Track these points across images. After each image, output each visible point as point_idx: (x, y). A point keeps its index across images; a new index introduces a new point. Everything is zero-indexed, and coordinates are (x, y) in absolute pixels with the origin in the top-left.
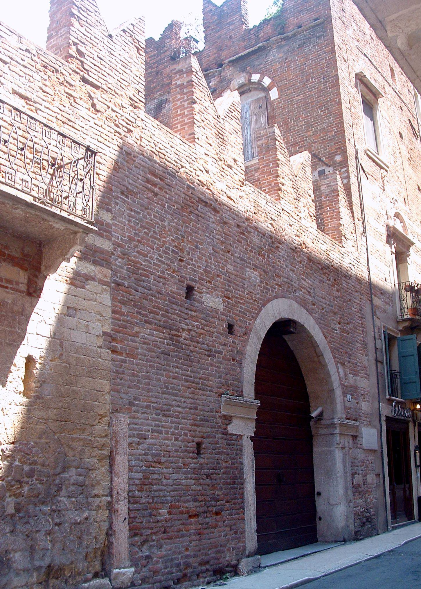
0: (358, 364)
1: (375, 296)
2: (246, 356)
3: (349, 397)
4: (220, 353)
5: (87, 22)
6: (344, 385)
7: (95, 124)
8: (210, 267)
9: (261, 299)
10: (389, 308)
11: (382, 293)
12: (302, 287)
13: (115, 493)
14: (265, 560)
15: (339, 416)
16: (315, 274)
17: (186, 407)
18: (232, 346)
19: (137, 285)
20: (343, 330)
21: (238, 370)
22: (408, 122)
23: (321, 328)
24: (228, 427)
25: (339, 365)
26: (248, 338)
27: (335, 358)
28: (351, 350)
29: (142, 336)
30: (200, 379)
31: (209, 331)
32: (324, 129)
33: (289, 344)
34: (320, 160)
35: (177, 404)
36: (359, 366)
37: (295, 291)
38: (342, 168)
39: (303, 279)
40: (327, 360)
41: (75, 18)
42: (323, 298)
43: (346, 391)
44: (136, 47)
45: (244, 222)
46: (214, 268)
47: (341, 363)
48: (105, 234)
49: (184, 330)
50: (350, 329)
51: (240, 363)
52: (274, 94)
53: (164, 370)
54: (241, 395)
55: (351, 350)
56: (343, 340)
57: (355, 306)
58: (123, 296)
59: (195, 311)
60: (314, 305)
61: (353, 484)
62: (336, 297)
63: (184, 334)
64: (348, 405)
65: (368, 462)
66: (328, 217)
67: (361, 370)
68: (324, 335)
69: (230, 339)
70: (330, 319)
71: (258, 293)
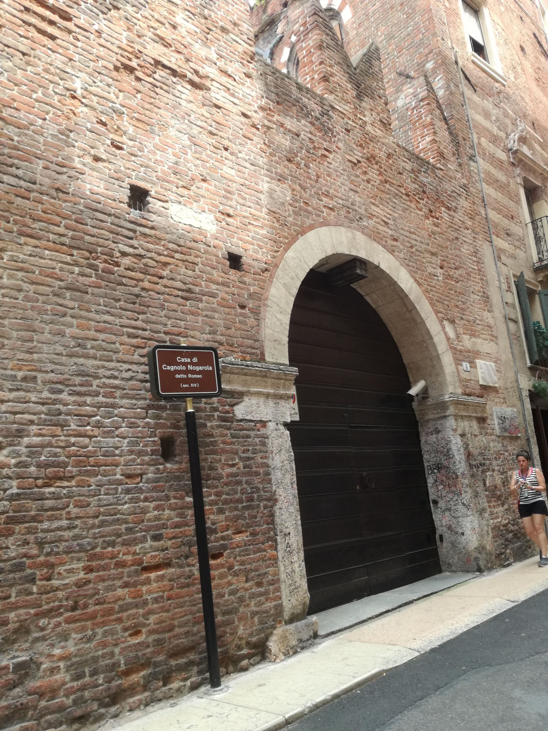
0: (478, 322)
1: (498, 236)
2: (269, 302)
3: (466, 365)
4: (214, 296)
6: (455, 349)
8: (185, 166)
9: (296, 225)
10: (521, 254)
11: (508, 234)
12: (371, 216)
14: (324, 620)
15: (452, 389)
16: (394, 200)
17: (131, 378)
18: (238, 287)
20: (449, 277)
21: (251, 321)
22: (533, 36)
23: (410, 272)
24: (235, 408)
25: (446, 323)
26: (271, 277)
27: (437, 312)
28: (464, 303)
29: (12, 256)
30: (166, 333)
31: (186, 261)
32: (409, 35)
33: (367, 298)
34: (408, 77)
35: (108, 373)
36: (478, 324)
37: (361, 218)
39: (374, 204)
40: (423, 315)
42: (410, 233)
43: (461, 357)
45: (256, 112)
46: (193, 168)
47: (448, 319)
49: (124, 254)
50: (461, 275)
51: (256, 312)
53: (73, 317)
54: (262, 359)
55: (464, 303)
56: (451, 289)
57: (466, 247)
59: (152, 228)
60: (396, 240)
61: (485, 484)
62: (433, 233)
63: (126, 261)
64: (464, 375)
65: (506, 454)
66: (417, 136)
67: (483, 329)
68: (416, 280)
69: (233, 275)
70: (424, 261)
71: (289, 216)
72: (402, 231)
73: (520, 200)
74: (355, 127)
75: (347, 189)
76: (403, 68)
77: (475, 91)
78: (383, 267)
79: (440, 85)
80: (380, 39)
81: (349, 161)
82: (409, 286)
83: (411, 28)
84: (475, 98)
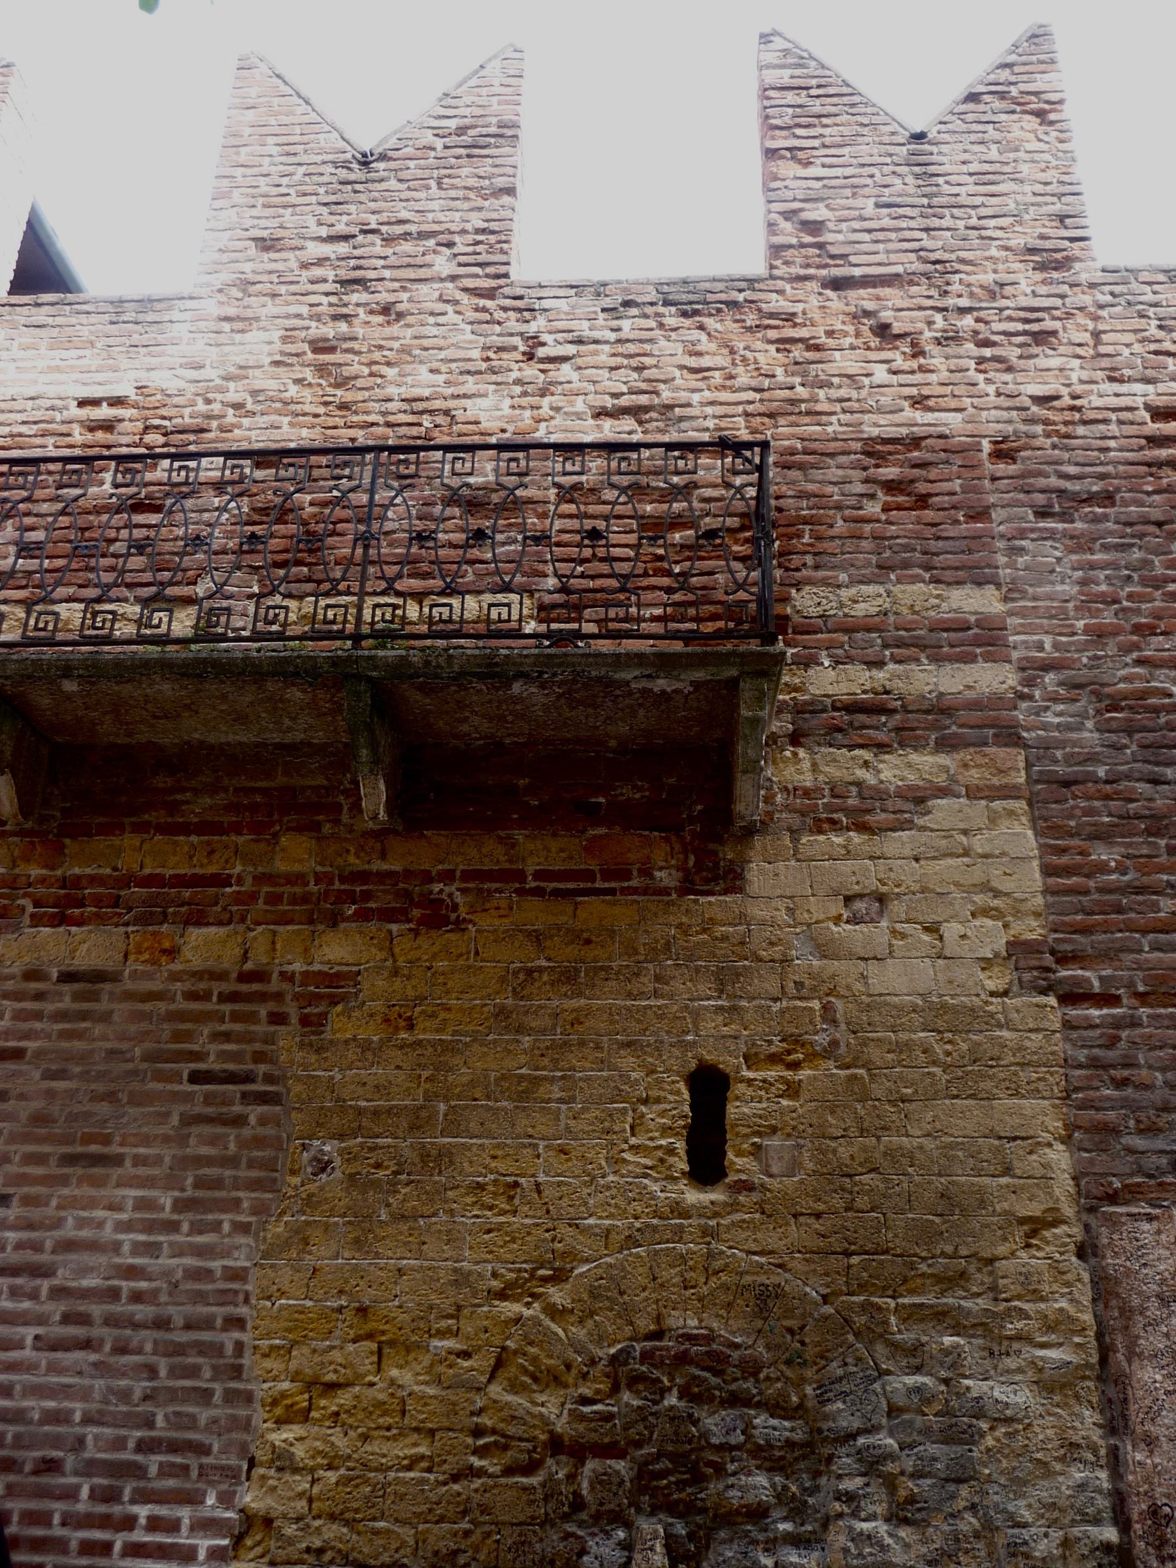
5: (824, 146)
7: (895, 373)
13: (1137, 1508)
19: (1157, 764)
41: (783, 157)
44: (1032, 113)
48: (978, 651)
58: (1089, 812)
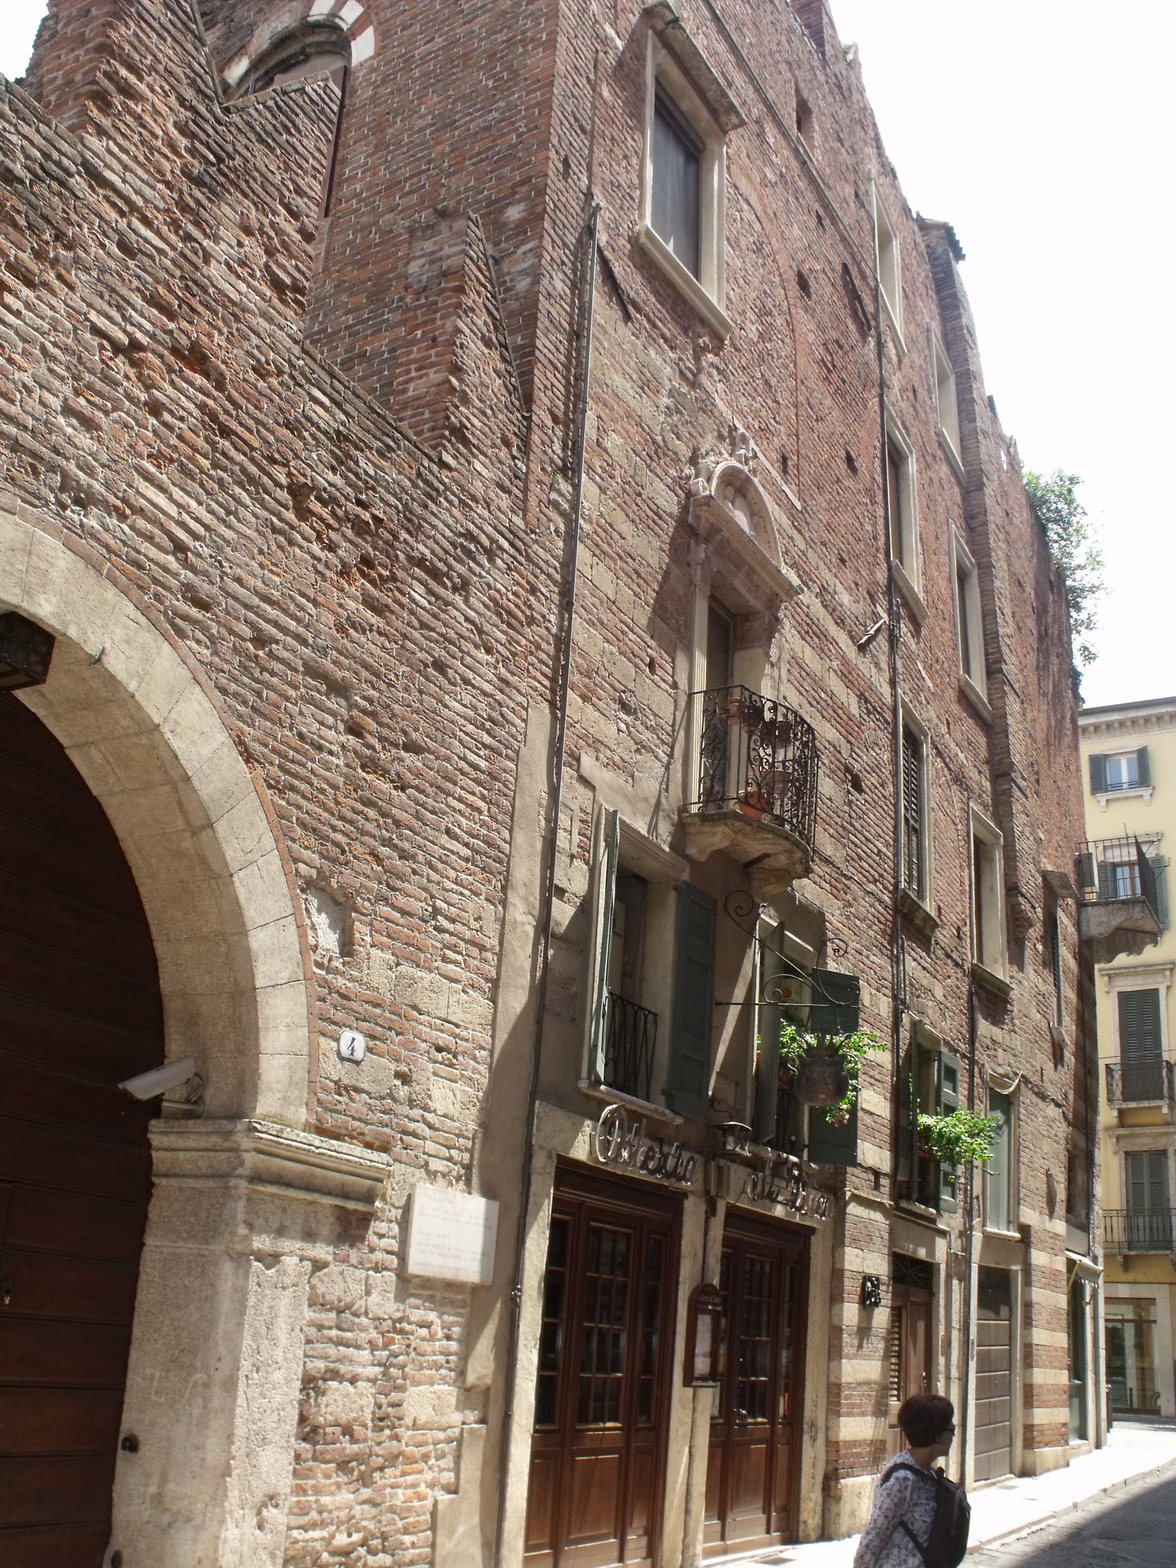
1: (585, 698)
3: (353, 1040)
11: (625, 707)
32: (487, 128)
38: (523, 243)
40: (231, 853)
52: (363, 48)
66: (410, 362)
68: (240, 743)
72: (235, 587)
73: (689, 626)
74: (160, 251)
75: (55, 403)
76: (452, 203)
77: (627, 317)
78: (115, 664)
79: (526, 265)
80: (421, 123)
81: (96, 331)
82: (206, 751)
83: (495, 114)
84: (624, 332)
